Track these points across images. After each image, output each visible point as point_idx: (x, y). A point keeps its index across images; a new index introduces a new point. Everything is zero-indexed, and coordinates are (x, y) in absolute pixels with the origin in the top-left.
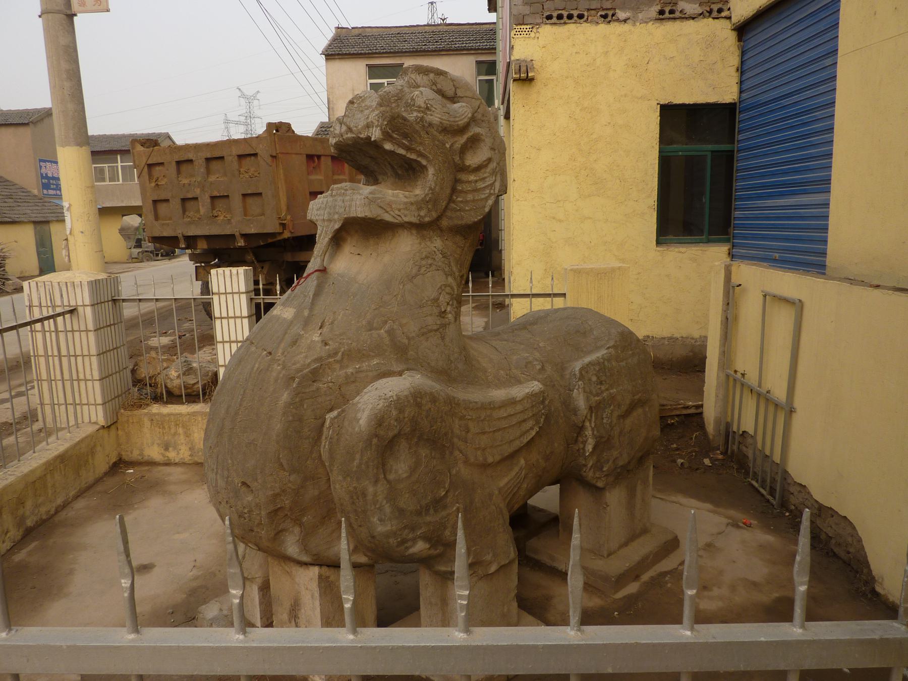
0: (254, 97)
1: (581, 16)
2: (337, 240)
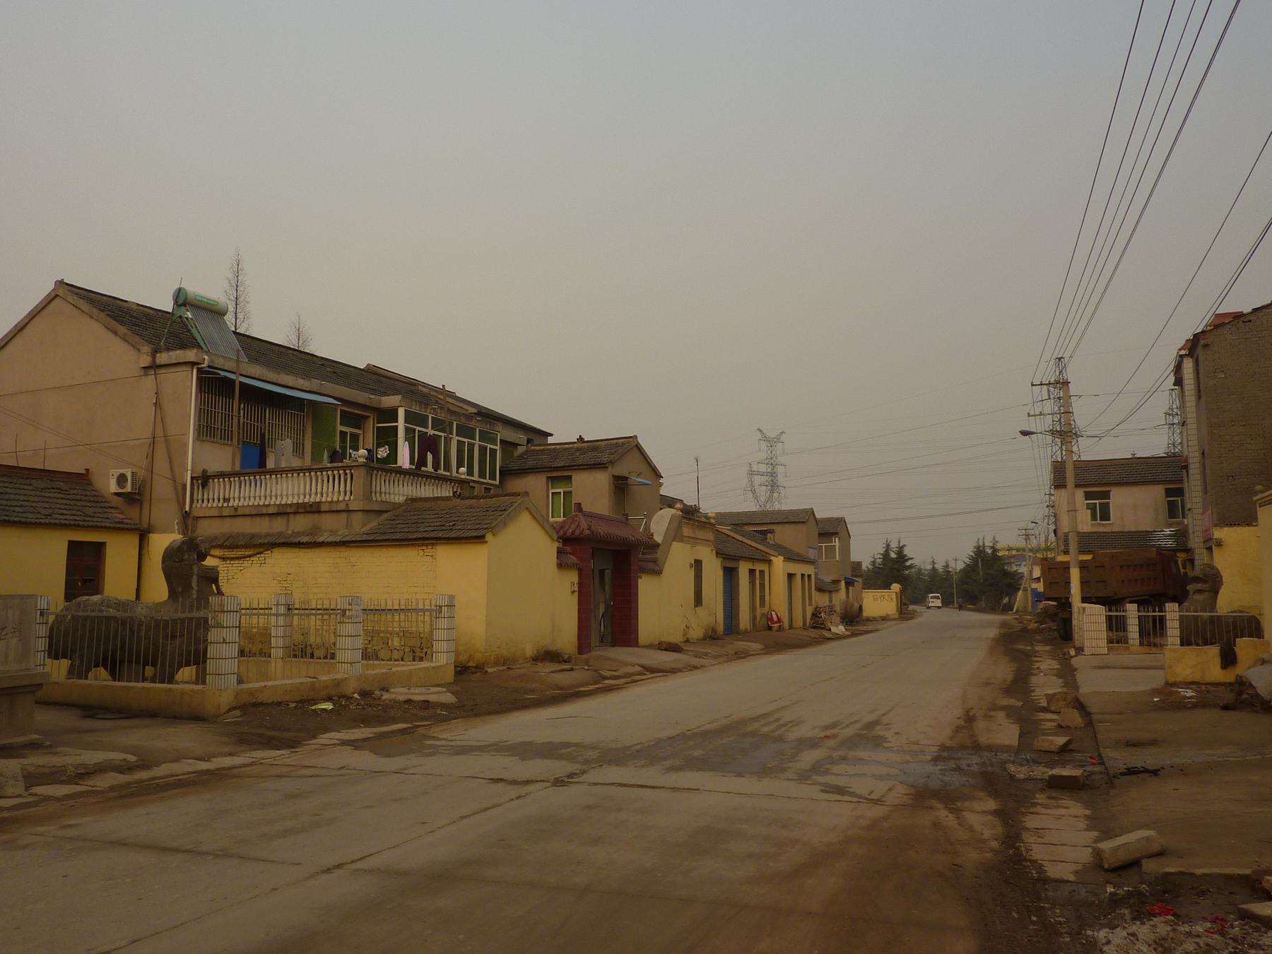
0: (778, 439)
1: (1239, 524)
2: (1194, 593)
